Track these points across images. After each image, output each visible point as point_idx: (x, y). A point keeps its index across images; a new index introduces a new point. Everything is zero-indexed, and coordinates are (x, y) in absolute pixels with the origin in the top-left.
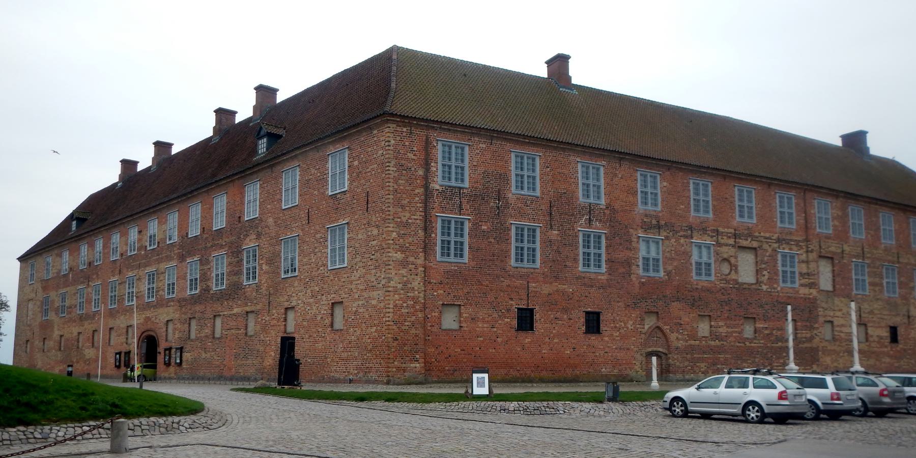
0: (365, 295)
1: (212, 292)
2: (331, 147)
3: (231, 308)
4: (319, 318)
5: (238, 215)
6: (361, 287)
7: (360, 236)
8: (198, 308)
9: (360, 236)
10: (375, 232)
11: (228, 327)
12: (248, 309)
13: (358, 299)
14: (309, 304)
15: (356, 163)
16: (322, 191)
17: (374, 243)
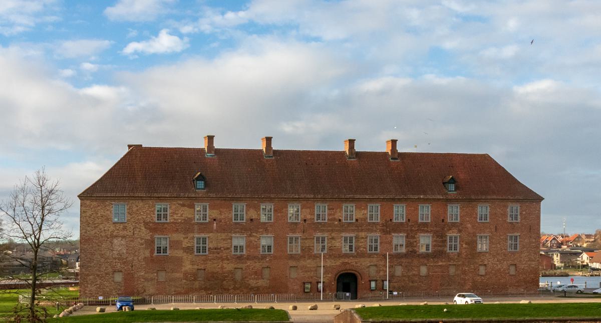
0: (529, 263)
1: (418, 253)
2: (509, 203)
3: (437, 262)
4: (502, 270)
5: (442, 218)
6: (527, 260)
7: (526, 241)
8: (404, 260)
9: (526, 241)
10: (534, 241)
11: (434, 271)
12: (451, 263)
13: (525, 264)
14: (497, 264)
15: (524, 213)
16: (504, 219)
17: (534, 244)
